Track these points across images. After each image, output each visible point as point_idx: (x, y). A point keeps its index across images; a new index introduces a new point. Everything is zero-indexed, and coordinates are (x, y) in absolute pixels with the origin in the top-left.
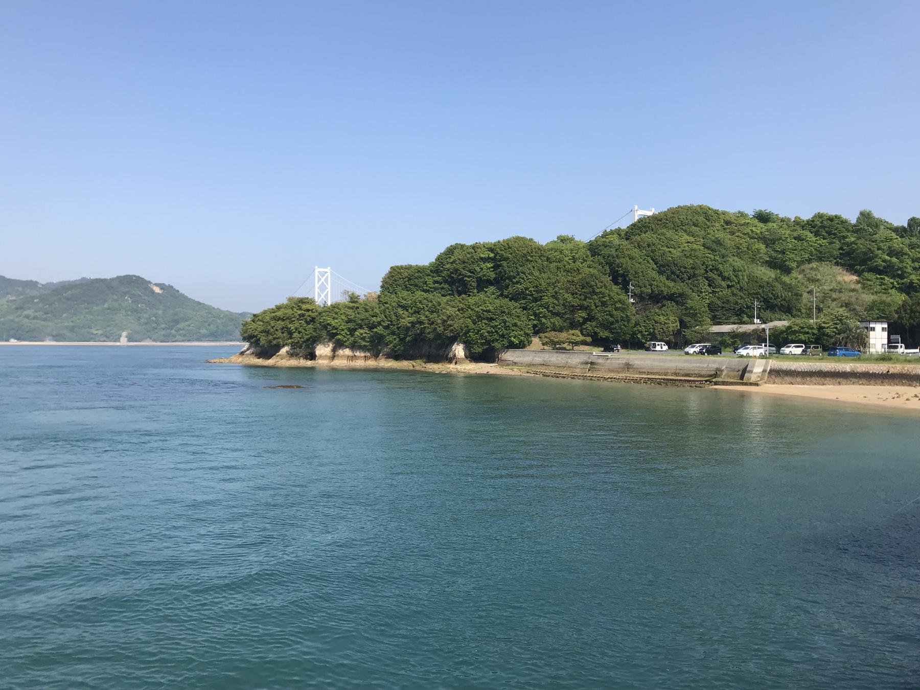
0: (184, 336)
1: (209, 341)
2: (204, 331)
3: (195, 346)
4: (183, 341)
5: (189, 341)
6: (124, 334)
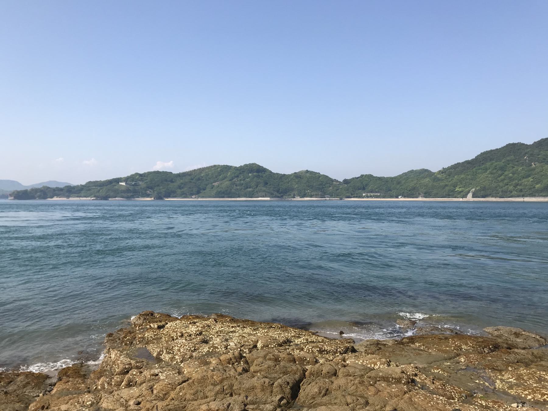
0: (521, 191)
1: (541, 196)
2: (537, 186)
3: (524, 202)
4: (518, 196)
5: (523, 196)
6: (474, 189)
